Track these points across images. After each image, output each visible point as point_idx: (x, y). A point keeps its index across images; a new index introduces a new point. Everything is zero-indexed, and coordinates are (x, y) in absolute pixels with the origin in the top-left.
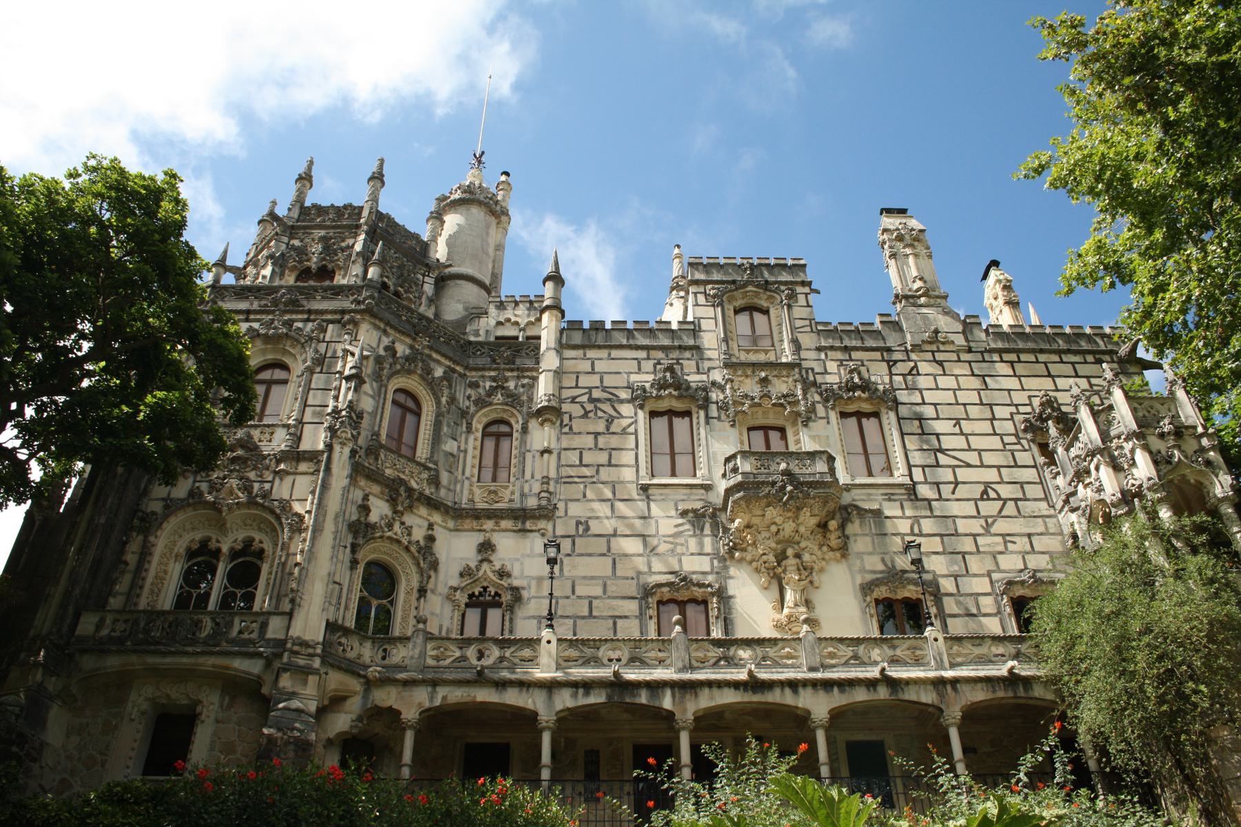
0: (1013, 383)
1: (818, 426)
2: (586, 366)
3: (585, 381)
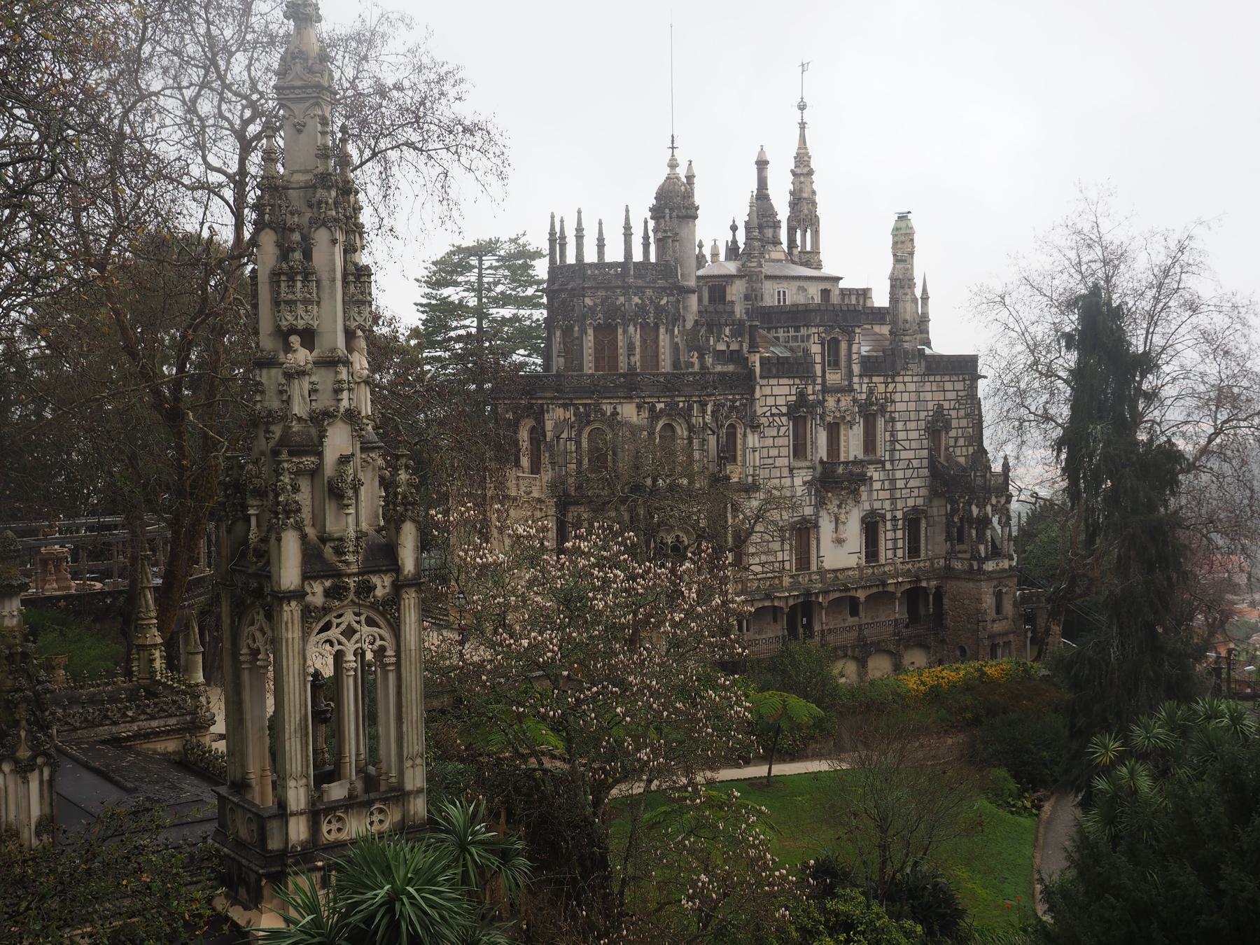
1: (855, 427)
2: (767, 391)
3: (770, 401)
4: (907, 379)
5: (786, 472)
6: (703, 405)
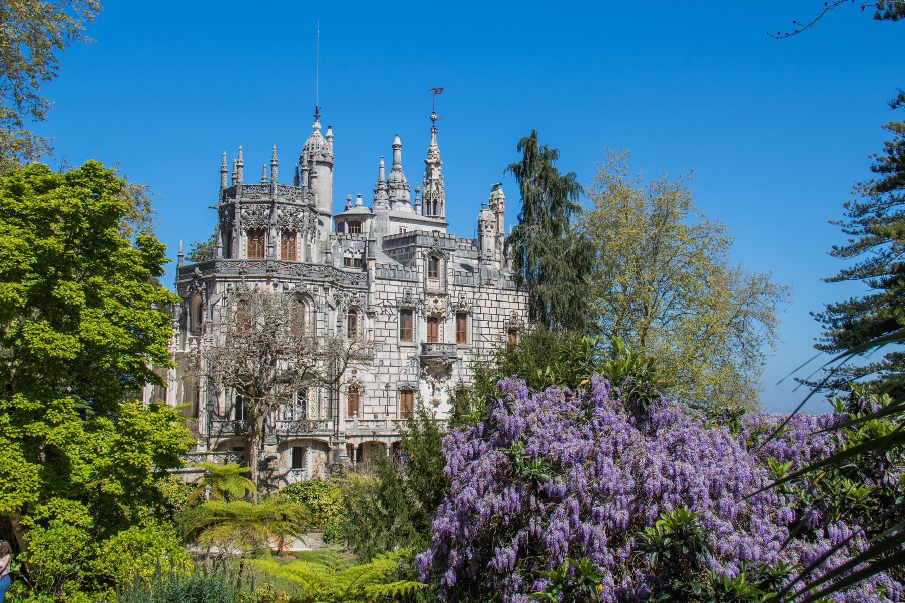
0: (506, 305)
2: (381, 288)
3: (383, 296)
4: (489, 291)
5: (394, 348)
6: (326, 289)
